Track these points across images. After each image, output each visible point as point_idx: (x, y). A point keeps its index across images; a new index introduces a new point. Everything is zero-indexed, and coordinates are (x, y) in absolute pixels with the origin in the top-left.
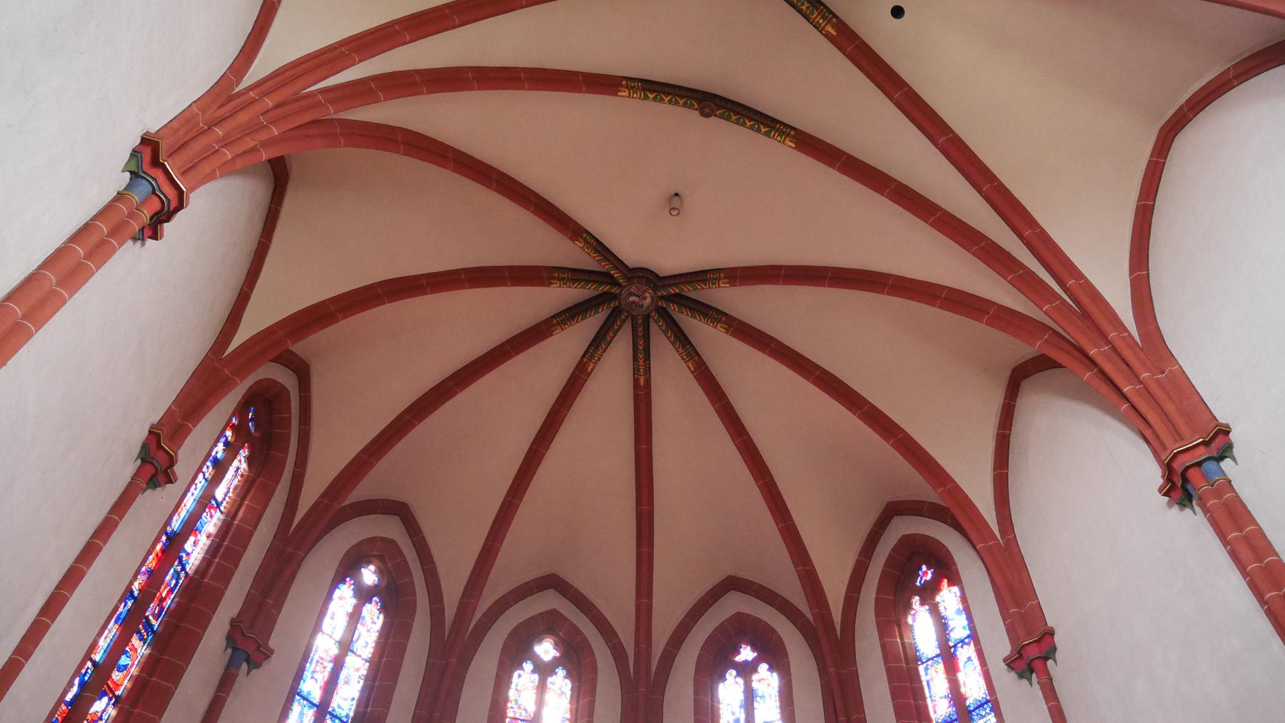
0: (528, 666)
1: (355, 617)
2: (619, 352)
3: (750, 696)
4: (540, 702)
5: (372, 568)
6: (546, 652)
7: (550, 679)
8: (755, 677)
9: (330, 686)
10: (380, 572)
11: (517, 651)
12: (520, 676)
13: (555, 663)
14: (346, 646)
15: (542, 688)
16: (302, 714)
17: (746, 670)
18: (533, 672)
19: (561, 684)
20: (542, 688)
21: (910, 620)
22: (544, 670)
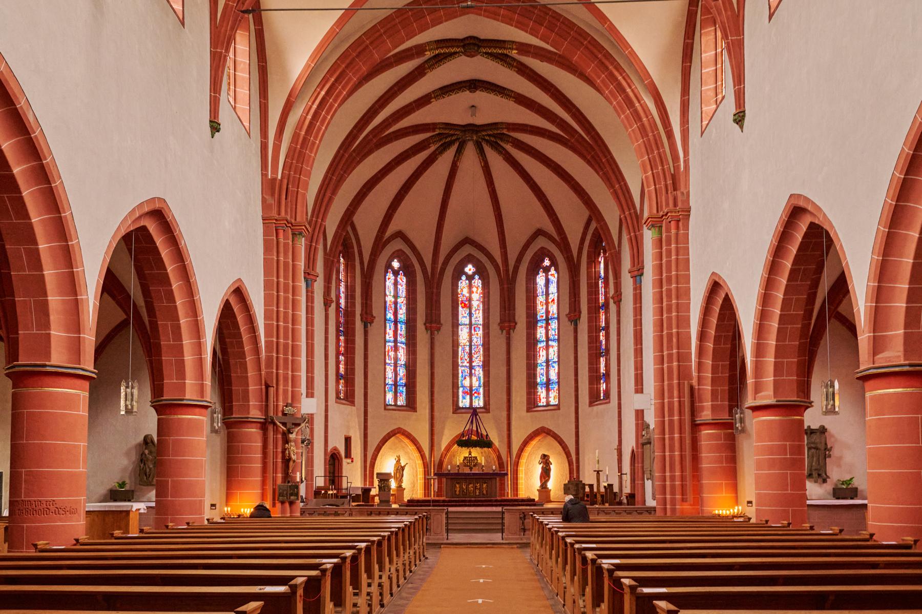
0: (464, 278)
1: (396, 284)
2: (470, 151)
3: (548, 282)
4: (471, 292)
5: (395, 260)
6: (470, 270)
7: (473, 281)
8: (550, 273)
9: (395, 313)
10: (399, 261)
11: (459, 273)
12: (461, 283)
13: (474, 274)
14: (396, 296)
15: (470, 286)
16: (390, 326)
17: (547, 270)
18: (466, 279)
19: (477, 282)
20: (470, 286)
21: (600, 260)
22: (470, 278)
